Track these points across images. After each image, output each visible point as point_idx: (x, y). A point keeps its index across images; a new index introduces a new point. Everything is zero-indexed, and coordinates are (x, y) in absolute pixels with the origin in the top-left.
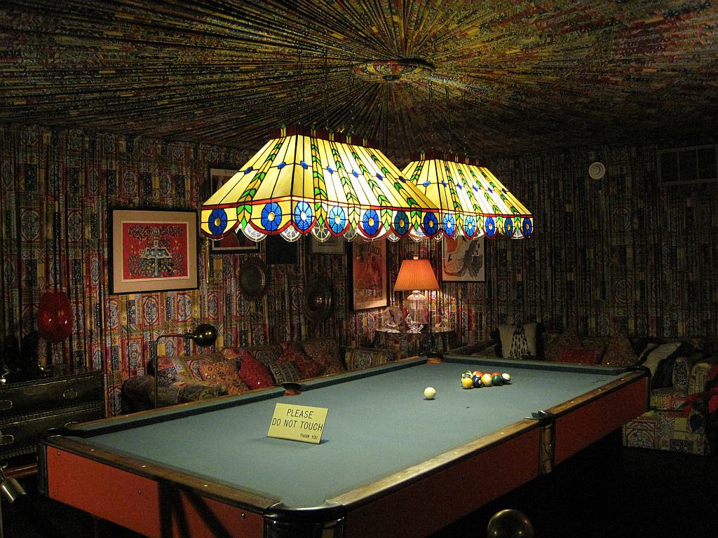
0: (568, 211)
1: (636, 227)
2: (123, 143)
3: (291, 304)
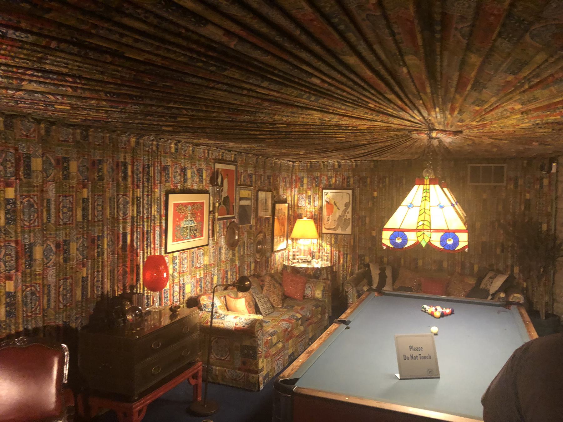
2: (173, 146)
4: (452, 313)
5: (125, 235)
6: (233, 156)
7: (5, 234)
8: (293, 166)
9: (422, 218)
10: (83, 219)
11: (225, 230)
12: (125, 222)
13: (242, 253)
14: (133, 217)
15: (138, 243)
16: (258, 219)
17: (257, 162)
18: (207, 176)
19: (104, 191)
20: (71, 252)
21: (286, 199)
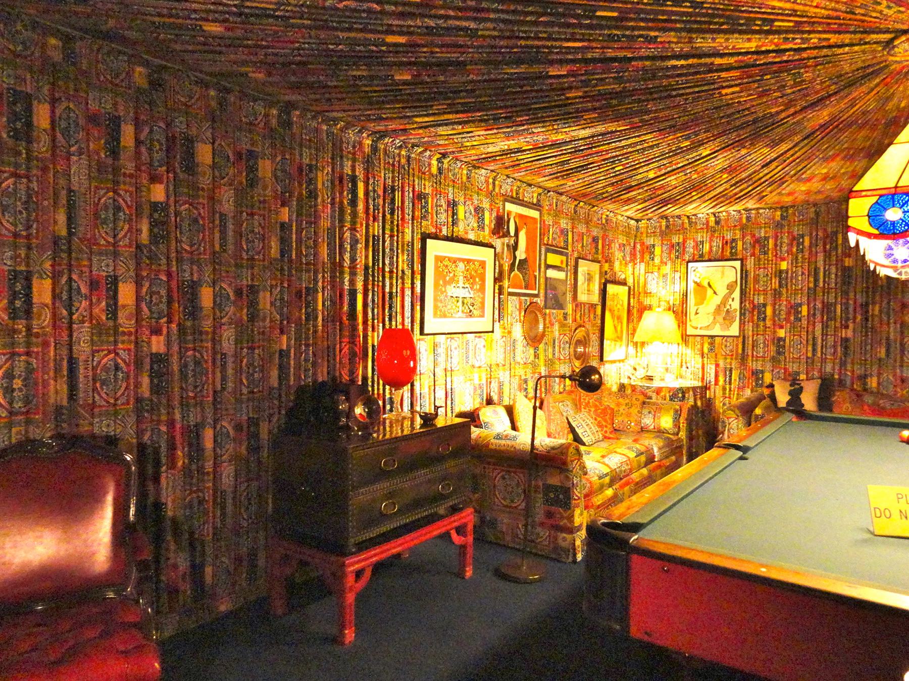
0: (847, 264)
2: (434, 162)
5: (353, 293)
6: (535, 195)
7: (149, 258)
8: (638, 228)
10: (282, 256)
11: (523, 313)
12: (353, 274)
13: (550, 356)
14: (366, 268)
15: (376, 310)
16: (578, 305)
17: (575, 212)
18: (491, 221)
19: (317, 217)
20: (261, 307)
21: (625, 279)
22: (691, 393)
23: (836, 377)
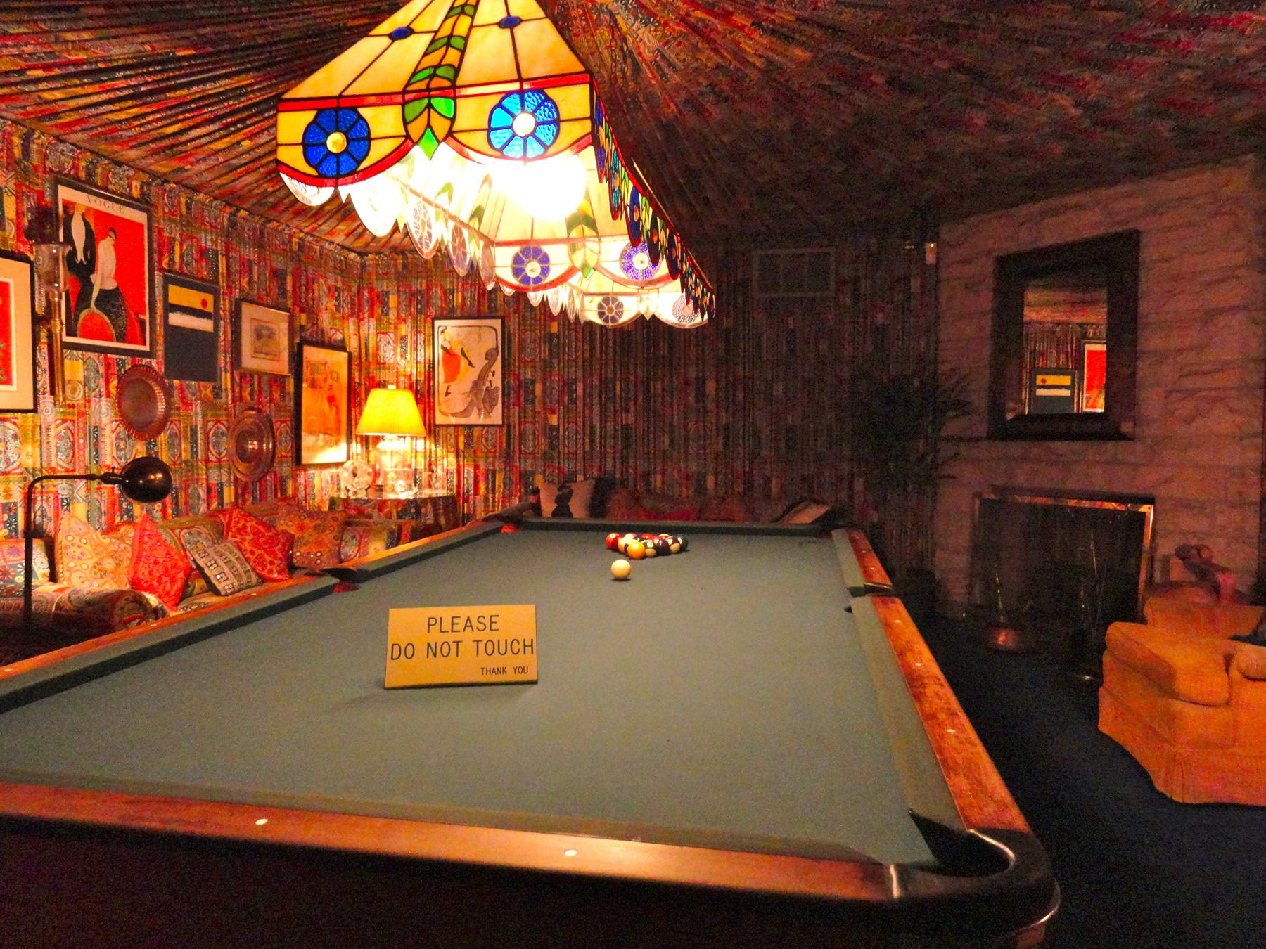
1: (721, 353)
3: (208, 450)
4: (683, 549)
8: (363, 266)
9: (433, 59)
18: (19, 214)
21: (343, 341)
22: (429, 506)
23: (618, 476)
